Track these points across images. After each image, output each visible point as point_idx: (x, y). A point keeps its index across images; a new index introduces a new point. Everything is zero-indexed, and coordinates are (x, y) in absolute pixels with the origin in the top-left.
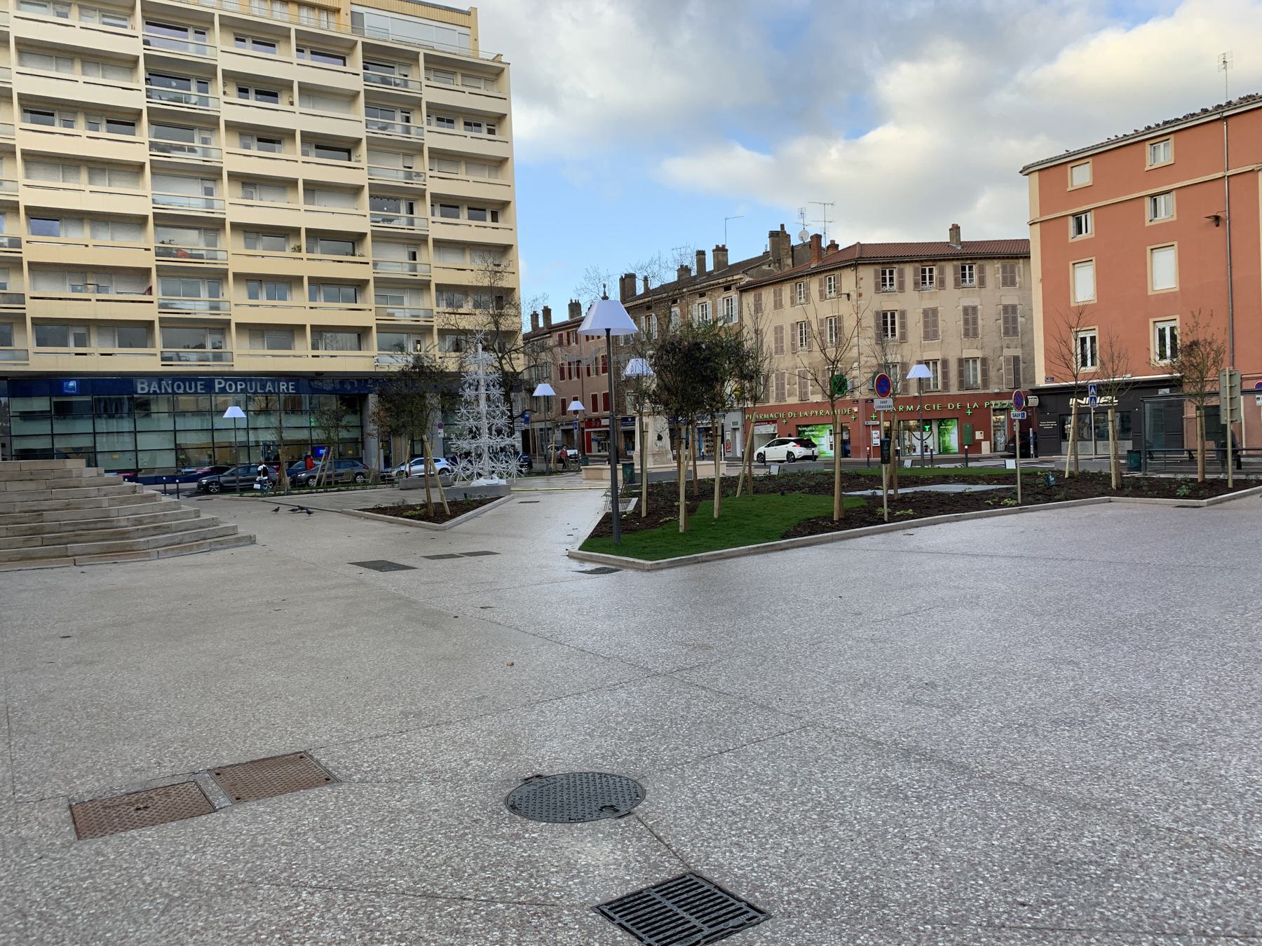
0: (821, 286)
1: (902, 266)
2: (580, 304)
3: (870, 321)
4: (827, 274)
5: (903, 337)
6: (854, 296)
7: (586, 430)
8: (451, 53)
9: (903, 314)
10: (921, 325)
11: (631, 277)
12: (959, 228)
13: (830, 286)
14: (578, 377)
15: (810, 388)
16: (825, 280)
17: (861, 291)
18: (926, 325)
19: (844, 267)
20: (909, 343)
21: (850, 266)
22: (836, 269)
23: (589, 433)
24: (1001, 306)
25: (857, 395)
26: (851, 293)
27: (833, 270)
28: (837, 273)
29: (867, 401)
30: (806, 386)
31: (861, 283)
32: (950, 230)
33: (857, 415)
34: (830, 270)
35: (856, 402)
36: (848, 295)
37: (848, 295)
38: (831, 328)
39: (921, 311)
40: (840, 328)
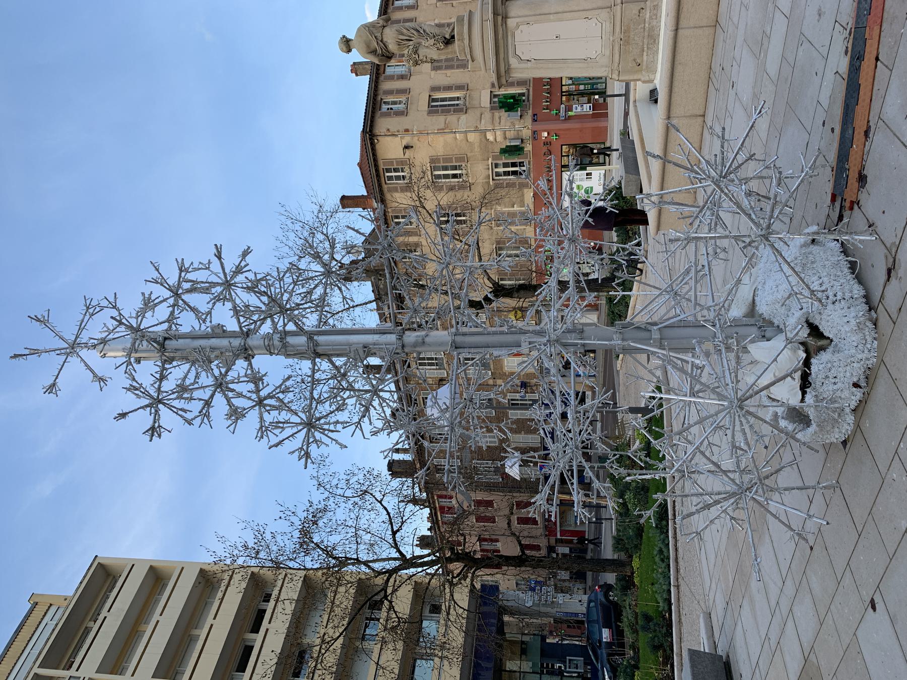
0: (396, 190)
1: (381, 92)
2: (422, 536)
3: (439, 120)
4: (383, 179)
5: (459, 88)
6: (407, 140)
7: (559, 537)
8: (54, 630)
9: (435, 89)
10: (449, 72)
11: (391, 465)
12: (354, 63)
13: (398, 178)
14: (497, 541)
15: (516, 208)
16: (390, 184)
17: (402, 129)
18: (451, 67)
19: (374, 155)
20: (469, 82)
21: (371, 139)
22: (376, 166)
23: (563, 533)
24: (438, 4)
25: (526, 133)
26: (404, 143)
27: (377, 170)
28: (381, 166)
29: (534, 120)
30: (512, 215)
31: (393, 129)
32: (357, 75)
33: (553, 133)
34: (378, 175)
35: (535, 134)
36: (406, 147)
37: (406, 147)
38: (446, 176)
39: (433, 72)
40: (445, 160)
